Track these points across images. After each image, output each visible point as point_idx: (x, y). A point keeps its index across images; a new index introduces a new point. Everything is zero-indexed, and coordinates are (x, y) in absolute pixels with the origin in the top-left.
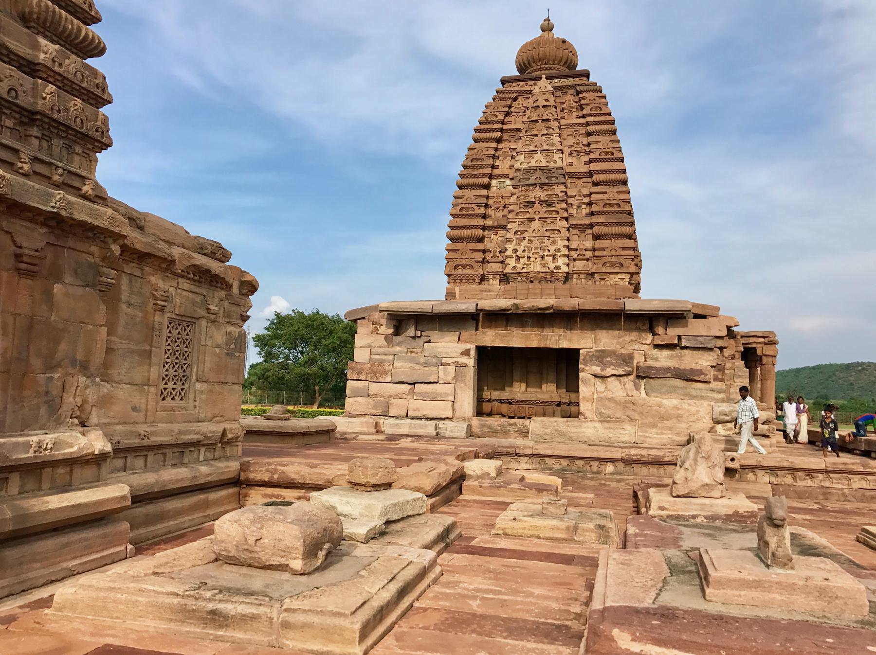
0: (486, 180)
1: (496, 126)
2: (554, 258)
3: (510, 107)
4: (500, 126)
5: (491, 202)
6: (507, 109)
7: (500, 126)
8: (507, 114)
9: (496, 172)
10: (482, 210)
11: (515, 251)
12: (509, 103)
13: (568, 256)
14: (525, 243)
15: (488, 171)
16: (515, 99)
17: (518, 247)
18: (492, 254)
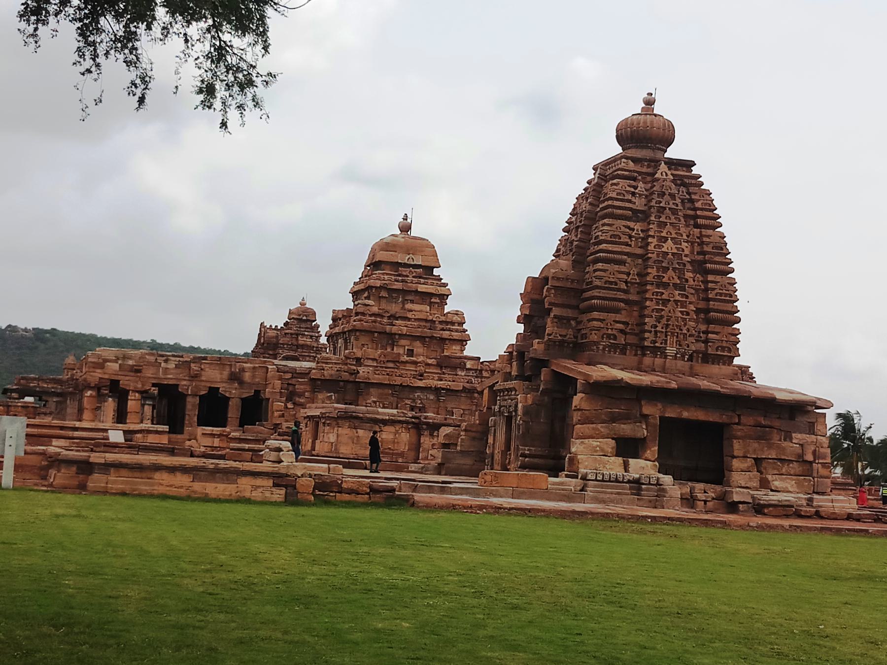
14: (664, 321)
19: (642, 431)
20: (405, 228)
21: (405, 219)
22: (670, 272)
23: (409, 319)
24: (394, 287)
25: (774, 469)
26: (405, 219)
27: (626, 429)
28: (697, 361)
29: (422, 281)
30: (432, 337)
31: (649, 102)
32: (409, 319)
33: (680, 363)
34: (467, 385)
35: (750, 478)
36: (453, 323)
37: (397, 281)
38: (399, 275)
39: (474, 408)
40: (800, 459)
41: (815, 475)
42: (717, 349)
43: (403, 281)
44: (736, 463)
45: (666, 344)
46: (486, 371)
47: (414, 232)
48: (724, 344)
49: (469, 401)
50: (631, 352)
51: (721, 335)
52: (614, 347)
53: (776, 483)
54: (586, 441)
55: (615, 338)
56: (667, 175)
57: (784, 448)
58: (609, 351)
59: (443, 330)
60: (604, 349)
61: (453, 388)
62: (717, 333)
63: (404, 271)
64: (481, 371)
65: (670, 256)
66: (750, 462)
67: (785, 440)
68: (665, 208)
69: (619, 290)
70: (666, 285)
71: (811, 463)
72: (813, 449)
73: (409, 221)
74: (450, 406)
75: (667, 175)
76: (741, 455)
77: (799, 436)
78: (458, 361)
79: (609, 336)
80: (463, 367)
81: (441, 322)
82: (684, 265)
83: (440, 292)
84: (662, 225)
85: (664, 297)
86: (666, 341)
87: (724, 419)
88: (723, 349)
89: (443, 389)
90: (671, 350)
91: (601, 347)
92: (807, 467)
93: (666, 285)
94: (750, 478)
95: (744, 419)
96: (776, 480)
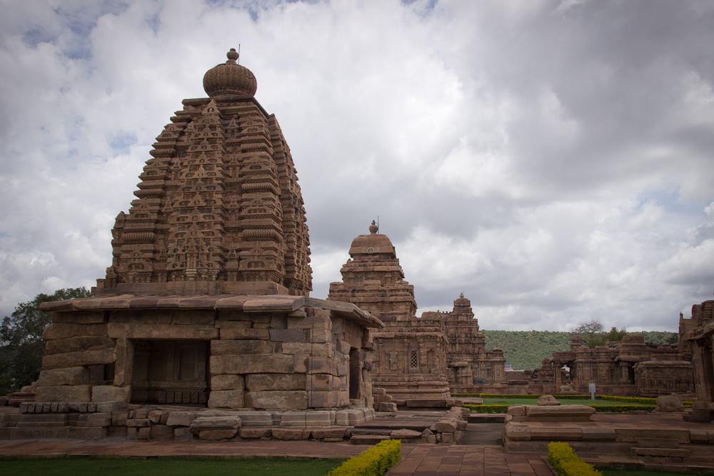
0: (160, 190)
1: (169, 143)
2: (208, 256)
3: (185, 127)
4: (174, 143)
5: (163, 210)
6: (181, 129)
7: (174, 143)
8: (182, 133)
9: (168, 183)
10: (155, 217)
11: (175, 251)
12: (184, 124)
13: (221, 256)
14: (185, 243)
15: (162, 182)
16: (189, 121)
17: (178, 247)
18: (160, 254)
19: (112, 357)
20: (374, 229)
21: (374, 223)
22: (198, 197)
23: (366, 291)
24: (358, 270)
25: (262, 384)
26: (374, 223)
27: (94, 355)
28: (232, 280)
29: (378, 263)
30: (383, 302)
31: (233, 56)
32: (366, 291)
33: (202, 284)
34: (398, 334)
35: (229, 396)
36: (399, 290)
37: (360, 266)
38: (363, 262)
39: (406, 350)
40: (290, 370)
41: (308, 387)
42: (249, 265)
43: (364, 266)
44: (215, 382)
45: (186, 266)
46: (414, 321)
47: (380, 232)
48: (256, 259)
49: (401, 345)
50: (162, 279)
51: (252, 250)
52: (143, 276)
53: (262, 401)
54: (50, 371)
55: (143, 267)
56: (213, 110)
57: (272, 361)
58: (140, 281)
59: (392, 296)
60: (134, 279)
61: (387, 336)
62: (248, 249)
63: (366, 258)
64: (410, 322)
65: (200, 182)
66: (230, 380)
67: (276, 351)
68: (203, 139)
69: (150, 221)
70: (191, 209)
71: (305, 374)
72: (305, 358)
73: (376, 225)
74: (387, 350)
75: (213, 110)
76: (220, 372)
77: (291, 345)
78: (391, 317)
79: (137, 266)
80: (394, 320)
81: (391, 290)
82: (215, 187)
83: (391, 270)
84: (197, 154)
85: (188, 221)
86: (186, 262)
87: (202, 334)
88: (257, 264)
89: (380, 338)
90: (191, 271)
91: (131, 277)
92: (301, 379)
93: (191, 209)
94: (229, 396)
95: (223, 334)
96: (261, 397)
